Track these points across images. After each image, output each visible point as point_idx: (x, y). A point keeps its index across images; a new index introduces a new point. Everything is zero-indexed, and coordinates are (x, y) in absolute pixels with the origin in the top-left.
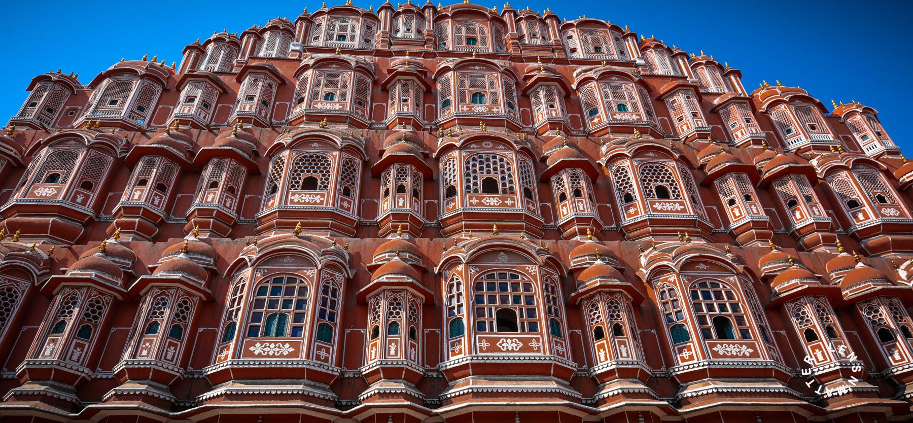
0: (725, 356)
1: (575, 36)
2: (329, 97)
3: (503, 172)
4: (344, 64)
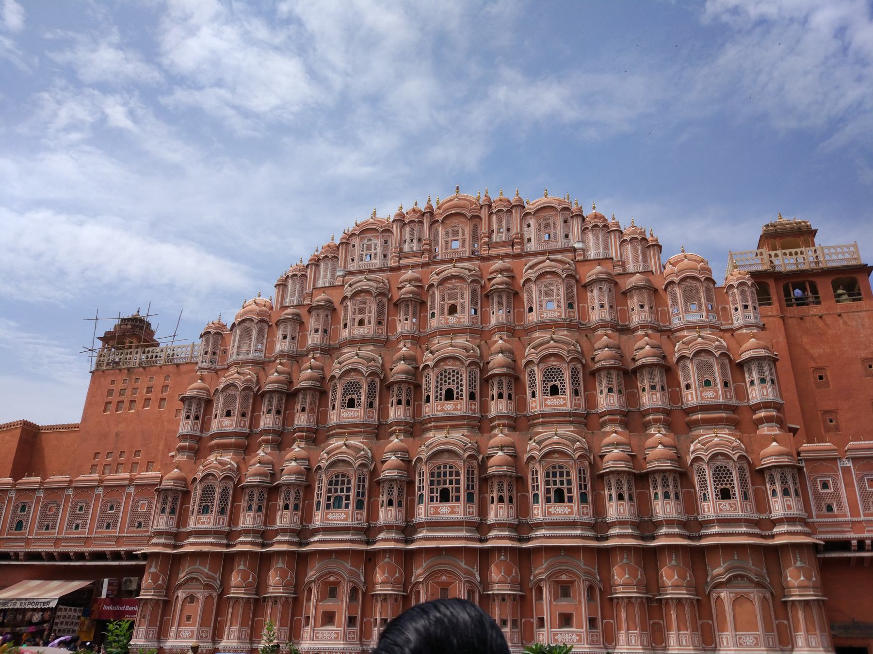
0: (554, 514)
1: (532, 225)
2: (361, 323)
3: (457, 383)
4: (367, 292)
